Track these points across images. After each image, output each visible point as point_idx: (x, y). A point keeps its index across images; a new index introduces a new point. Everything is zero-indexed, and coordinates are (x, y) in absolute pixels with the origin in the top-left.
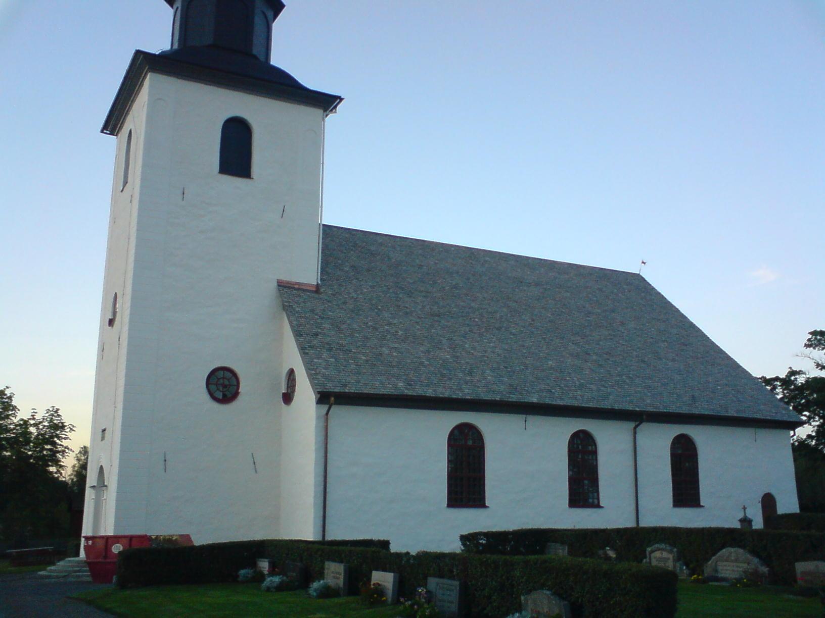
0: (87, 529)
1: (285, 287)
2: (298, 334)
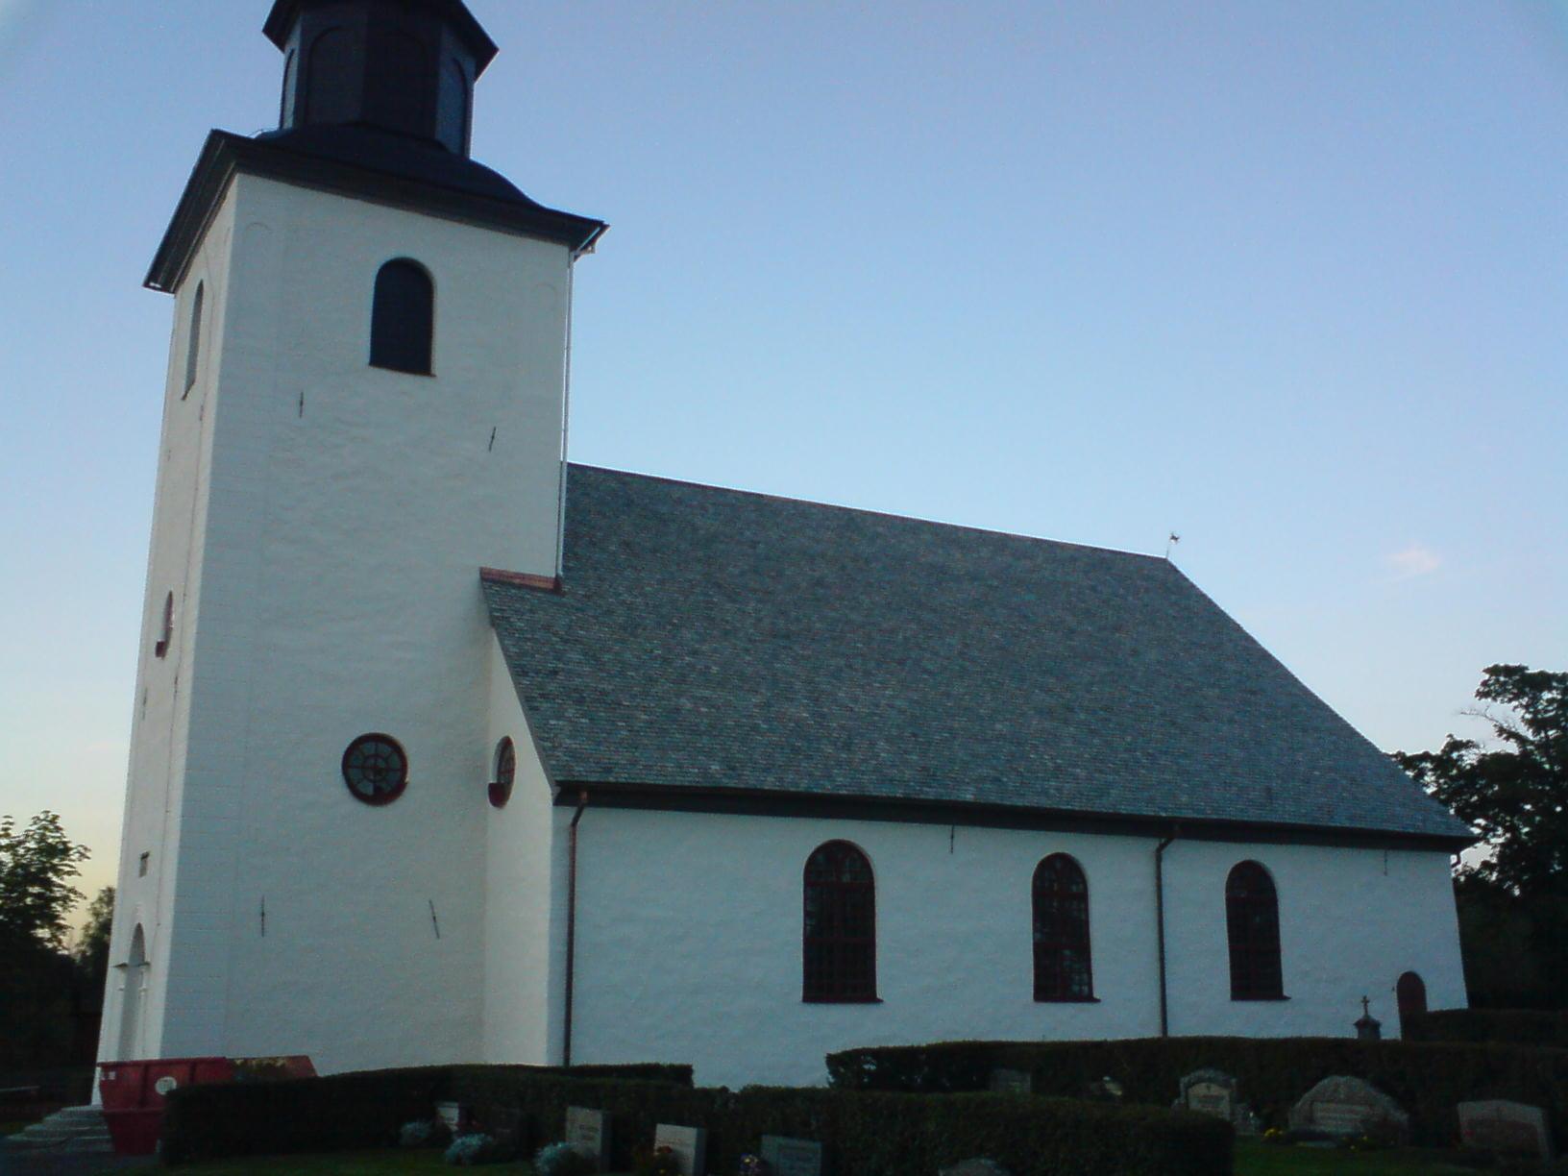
0: (108, 1050)
1: (494, 582)
2: (519, 671)
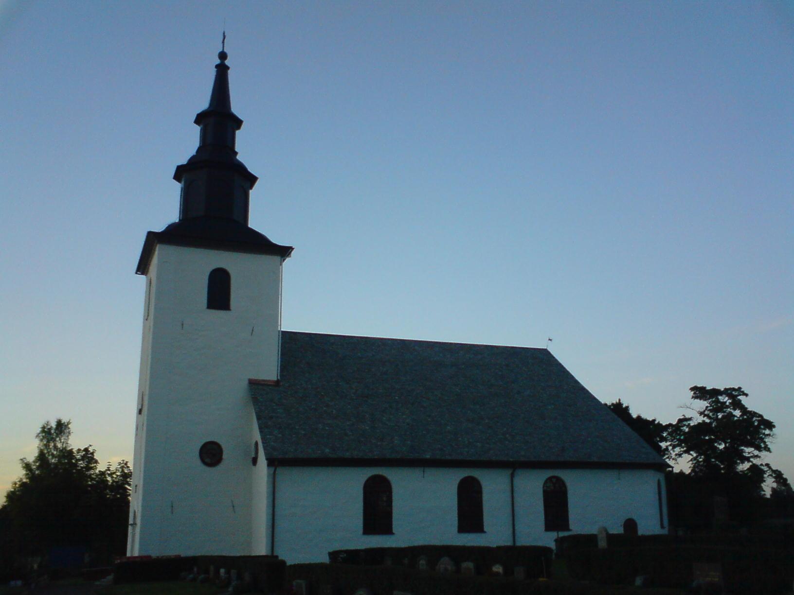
0: (128, 554)
1: (254, 384)
2: (259, 419)
